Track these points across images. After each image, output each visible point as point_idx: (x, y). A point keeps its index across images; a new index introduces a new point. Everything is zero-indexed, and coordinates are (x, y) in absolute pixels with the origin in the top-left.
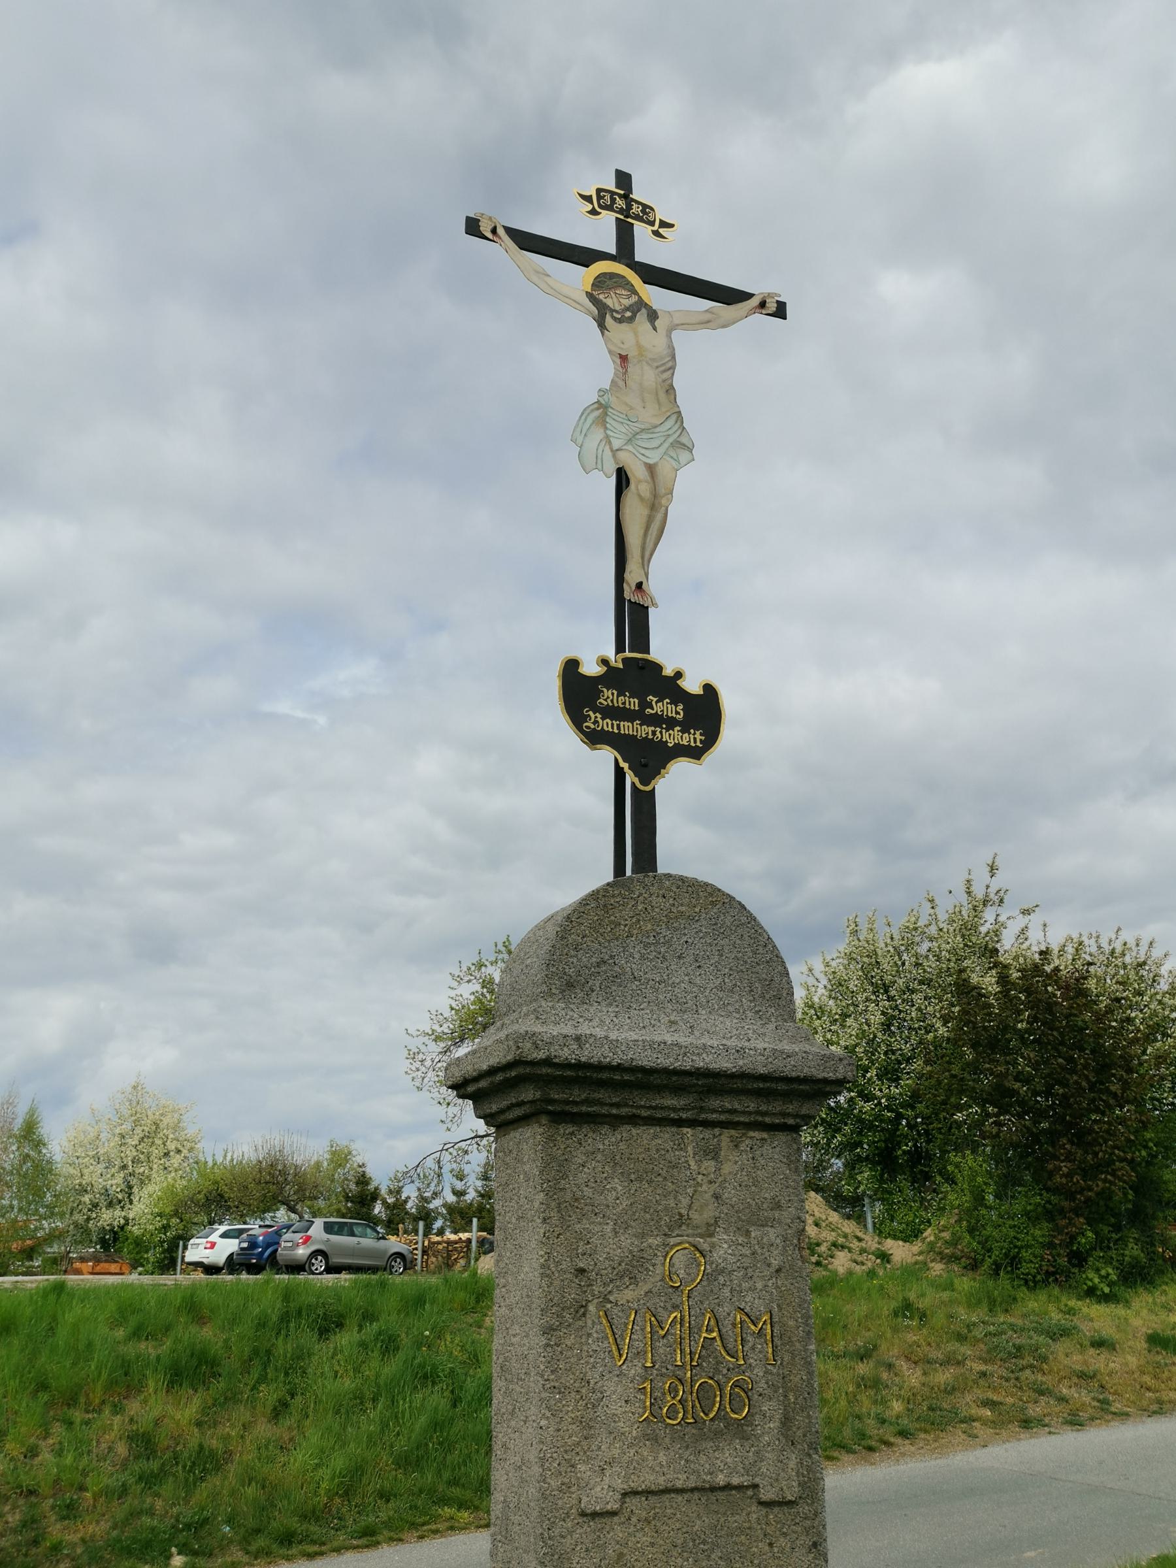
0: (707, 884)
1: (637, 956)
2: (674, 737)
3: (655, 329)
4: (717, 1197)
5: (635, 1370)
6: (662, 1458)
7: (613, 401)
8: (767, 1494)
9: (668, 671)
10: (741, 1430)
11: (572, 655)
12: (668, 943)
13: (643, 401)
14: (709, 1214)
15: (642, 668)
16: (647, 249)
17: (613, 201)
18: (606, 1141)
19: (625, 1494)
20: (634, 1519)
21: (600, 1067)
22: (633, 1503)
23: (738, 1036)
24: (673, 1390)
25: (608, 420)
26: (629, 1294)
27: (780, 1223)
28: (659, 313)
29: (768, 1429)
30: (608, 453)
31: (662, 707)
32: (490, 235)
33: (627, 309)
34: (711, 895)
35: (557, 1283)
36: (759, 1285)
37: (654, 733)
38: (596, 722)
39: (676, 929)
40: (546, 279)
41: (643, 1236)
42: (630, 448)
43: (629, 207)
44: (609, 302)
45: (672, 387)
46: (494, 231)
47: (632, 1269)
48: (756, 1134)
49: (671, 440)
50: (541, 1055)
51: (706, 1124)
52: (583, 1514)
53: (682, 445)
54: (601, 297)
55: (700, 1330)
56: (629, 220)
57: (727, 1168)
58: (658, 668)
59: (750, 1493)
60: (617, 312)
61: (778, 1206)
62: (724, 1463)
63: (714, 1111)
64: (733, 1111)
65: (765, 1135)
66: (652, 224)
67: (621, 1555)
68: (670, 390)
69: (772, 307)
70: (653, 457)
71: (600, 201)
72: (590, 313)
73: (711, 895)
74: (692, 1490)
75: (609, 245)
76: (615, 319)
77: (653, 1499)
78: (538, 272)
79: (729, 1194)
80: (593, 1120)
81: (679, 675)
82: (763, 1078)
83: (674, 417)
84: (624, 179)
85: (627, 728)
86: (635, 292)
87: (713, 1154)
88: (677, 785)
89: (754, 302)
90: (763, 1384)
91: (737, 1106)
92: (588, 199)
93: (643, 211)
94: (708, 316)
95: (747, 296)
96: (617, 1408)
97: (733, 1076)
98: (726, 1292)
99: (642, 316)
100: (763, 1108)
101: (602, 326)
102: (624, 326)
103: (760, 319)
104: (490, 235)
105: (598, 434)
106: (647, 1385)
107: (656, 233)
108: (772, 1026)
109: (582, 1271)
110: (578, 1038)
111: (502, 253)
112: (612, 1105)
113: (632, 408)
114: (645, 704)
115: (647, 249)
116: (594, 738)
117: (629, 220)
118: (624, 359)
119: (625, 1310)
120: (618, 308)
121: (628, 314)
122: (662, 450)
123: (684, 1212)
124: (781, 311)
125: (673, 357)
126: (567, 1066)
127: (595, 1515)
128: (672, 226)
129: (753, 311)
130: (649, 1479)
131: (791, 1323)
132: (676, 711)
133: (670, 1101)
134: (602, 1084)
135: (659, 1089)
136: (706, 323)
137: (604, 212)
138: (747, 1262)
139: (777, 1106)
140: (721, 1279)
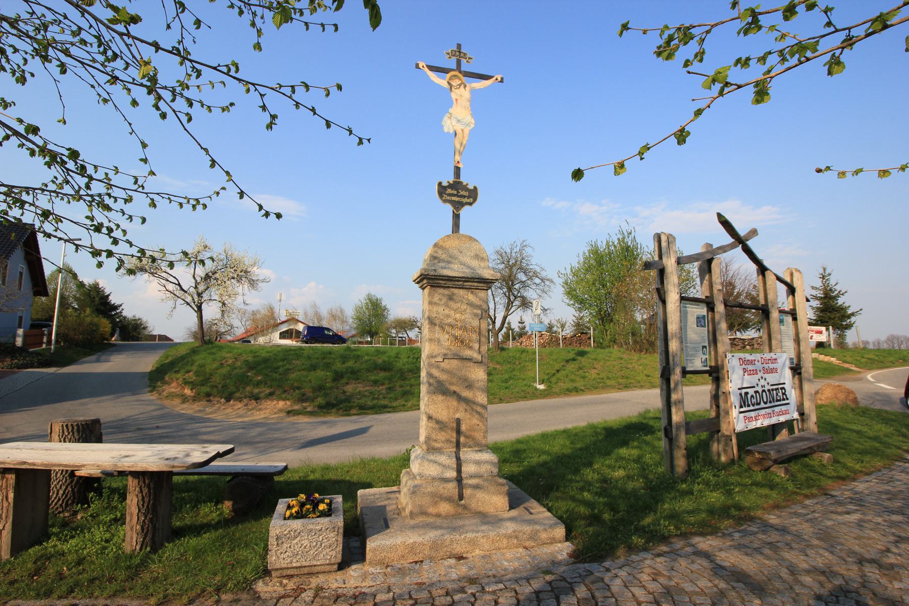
2: (465, 200)
16: (464, 68)
71: (453, 54)
75: (454, 66)
84: (459, 46)
85: (453, 198)
88: (465, 212)
116: (445, 201)
132: (466, 194)
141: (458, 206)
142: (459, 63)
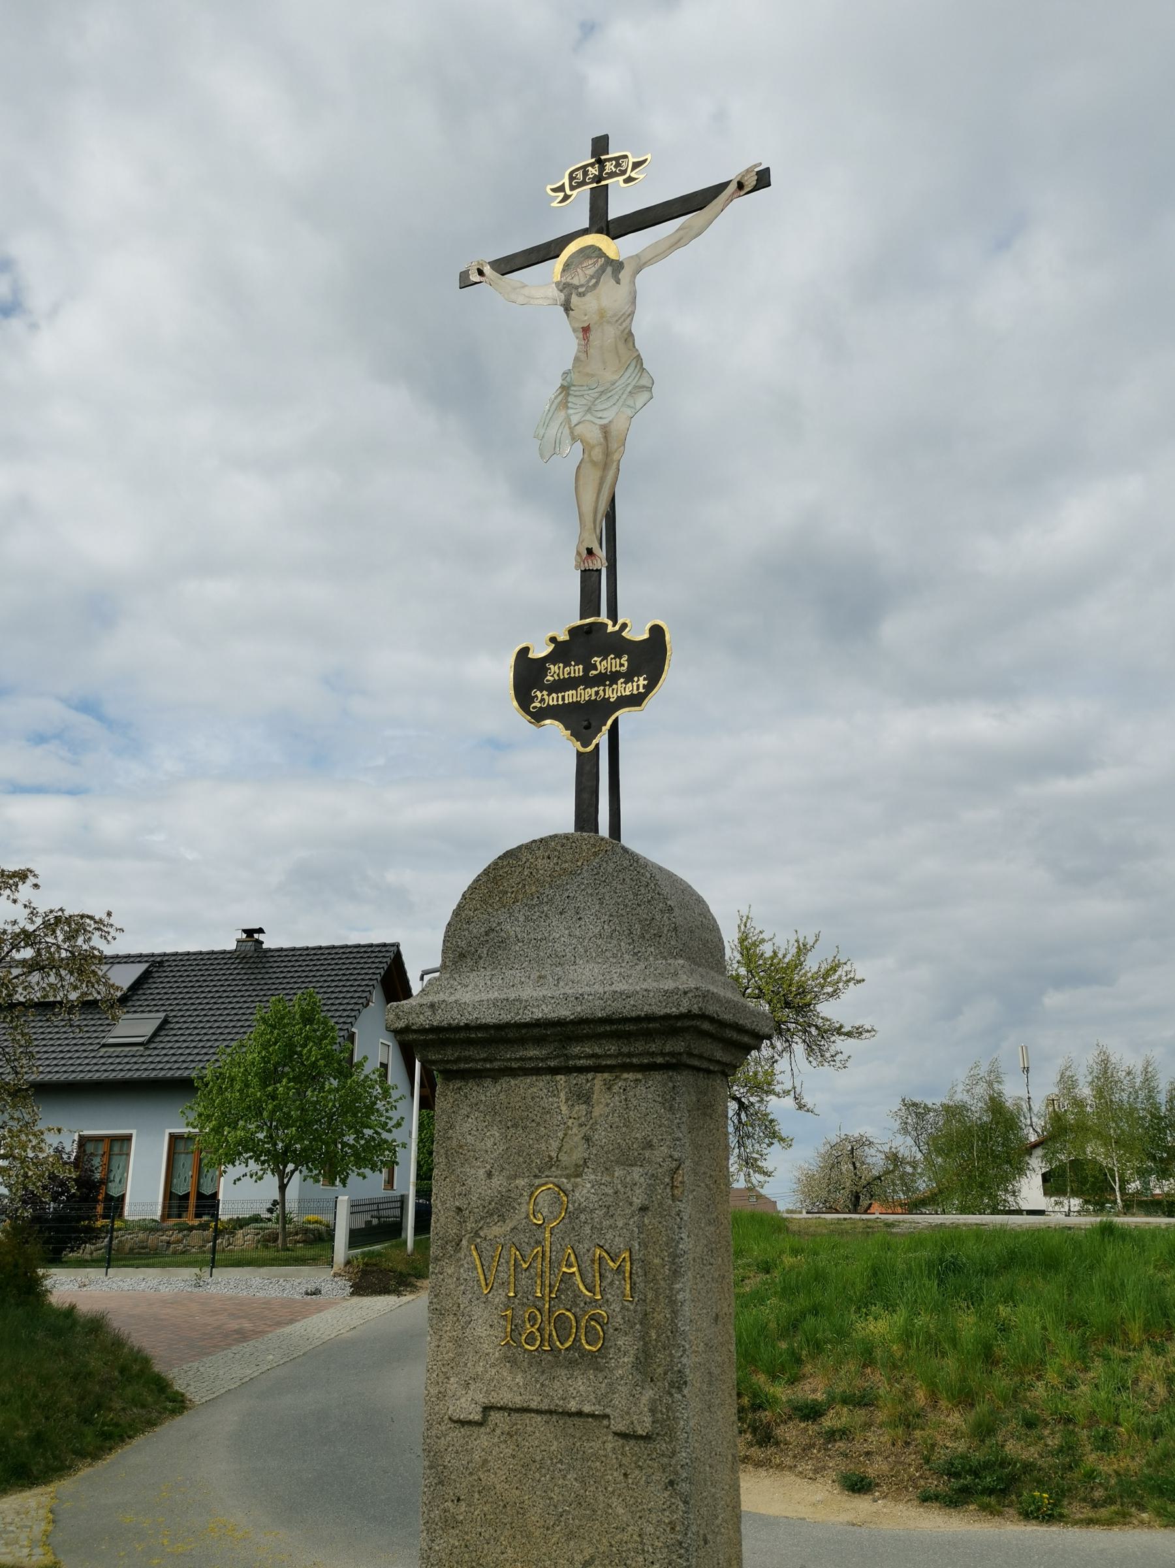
2: (612, 693)
3: (618, 282)
4: (587, 1139)
5: (499, 1298)
8: (621, 1427)
10: (595, 1362)
14: (579, 1154)
17: (585, 174)
18: (489, 1092)
20: (498, 1432)
21: (451, 1029)
22: (495, 1416)
26: (496, 1230)
29: (623, 1362)
31: (603, 665)
33: (592, 277)
36: (620, 1224)
38: (543, 700)
39: (558, 887)
41: (515, 1177)
45: (631, 334)
47: (501, 1207)
48: (630, 1076)
49: (629, 389)
56: (603, 183)
57: (597, 1112)
59: (605, 1422)
60: (582, 286)
61: (649, 1145)
62: (578, 1391)
64: (594, 1056)
65: (639, 1076)
67: (485, 1461)
68: (629, 337)
69: (751, 181)
70: (608, 416)
77: (515, 1416)
79: (600, 1136)
80: (477, 1075)
84: (600, 145)
85: (570, 696)
87: (584, 1097)
89: (733, 187)
90: (619, 1319)
91: (598, 1050)
93: (618, 165)
95: (723, 186)
97: (572, 1022)
100: (625, 1050)
109: (459, 1209)
114: (590, 667)
116: (538, 716)
117: (603, 183)
120: (583, 281)
121: (594, 281)
123: (554, 1154)
124: (763, 179)
130: (505, 1397)
131: (657, 1261)
132: (621, 664)
133: (532, 1052)
134: (470, 1042)
135: (522, 1042)
136: (677, 243)
137: (575, 193)
139: (639, 1046)
140: (583, 1217)
141: (585, 721)
142: (599, 199)
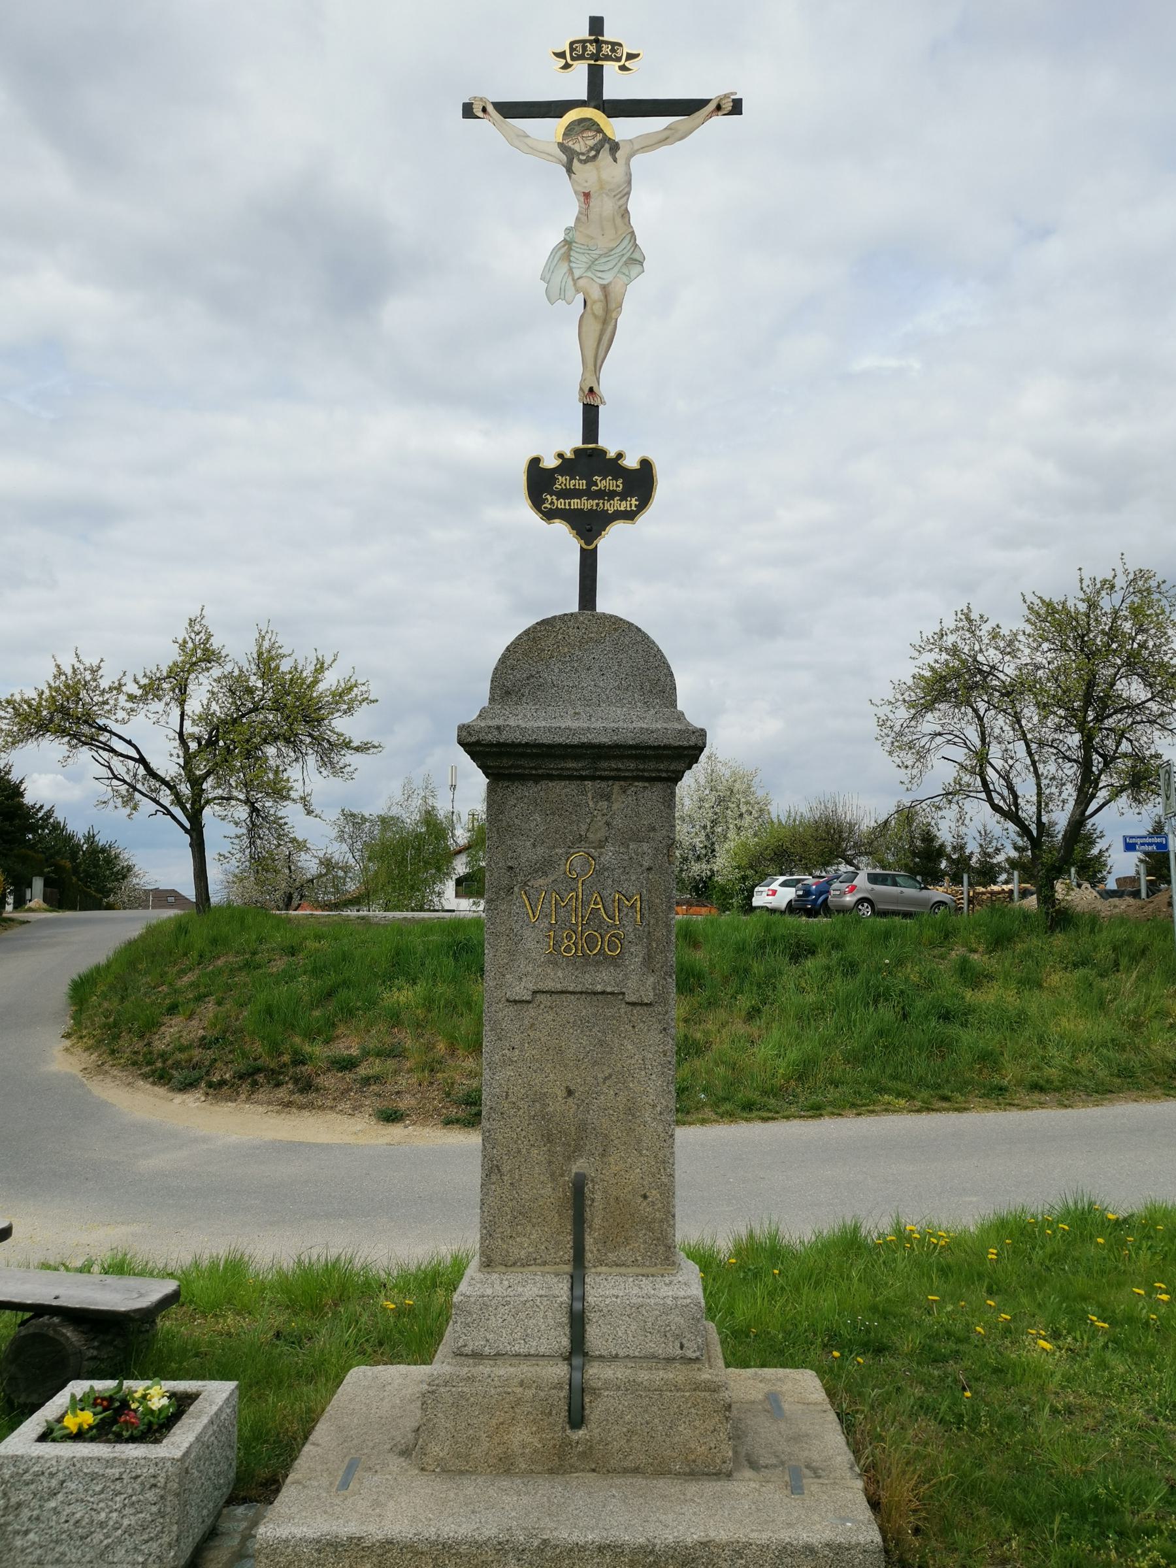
0: (611, 616)
1: (556, 671)
3: (615, 161)
4: (608, 824)
5: (544, 924)
6: (560, 974)
7: (579, 238)
8: (633, 999)
9: (612, 454)
10: (615, 962)
11: (534, 455)
12: (580, 660)
13: (603, 229)
14: (601, 835)
15: (590, 456)
16: (610, 92)
17: (584, 48)
18: (530, 790)
19: (535, 992)
20: (542, 1006)
21: (514, 745)
22: (539, 997)
23: (624, 720)
24: (569, 937)
25: (572, 253)
26: (541, 881)
27: (653, 840)
28: (621, 145)
29: (634, 962)
30: (570, 283)
31: (603, 483)
32: (480, 114)
33: (592, 149)
34: (614, 623)
35: (496, 875)
36: (633, 878)
37: (597, 505)
38: (552, 503)
39: (586, 650)
40: (527, 140)
41: (554, 847)
42: (589, 274)
43: (599, 49)
44: (577, 147)
45: (627, 211)
46: (484, 110)
47: (544, 867)
48: (640, 784)
49: (624, 259)
50: (473, 739)
51: (602, 778)
52: (508, 1001)
53: (635, 261)
54: (570, 144)
55: (589, 903)
56: (599, 63)
57: (615, 807)
58: (603, 452)
59: (621, 997)
60: (583, 154)
61: (654, 829)
62: (604, 979)
63: (605, 770)
64: (618, 770)
65: (647, 784)
66: (619, 59)
67: (533, 1025)
68: (625, 214)
69: (728, 106)
70: (608, 278)
71: (577, 51)
72: (560, 162)
73: (614, 623)
74: (581, 993)
75: (580, 92)
76: (580, 161)
77: (554, 996)
78: (518, 136)
79: (618, 822)
80: (522, 778)
81: (620, 456)
82: (631, 747)
83: (628, 237)
84: (596, 24)
85: (576, 503)
86: (600, 131)
87: (608, 797)
88: (614, 541)
89: (711, 106)
90: (632, 936)
91: (620, 766)
92: (561, 55)
93: (613, 50)
94: (668, 133)
95: (705, 102)
96: (531, 945)
97: (609, 747)
98: (610, 882)
99: (605, 154)
100: (641, 767)
101: (570, 171)
102: (589, 166)
103: (719, 121)
104: (480, 114)
105: (564, 268)
106: (552, 933)
107: (623, 68)
108: (652, 712)
109: (511, 868)
110: (498, 728)
111: (487, 127)
112: (531, 768)
113: (592, 238)
114: (592, 483)
115: (616, 86)
116: (549, 515)
117: (599, 63)
118: (587, 195)
119: (538, 890)
120: (584, 150)
121: (593, 153)
122: (616, 269)
123: (583, 833)
124: (737, 108)
125: (629, 182)
126: (491, 745)
127: (516, 1002)
128: (638, 55)
129: (710, 116)
130: (550, 985)
131: (657, 901)
132: (618, 485)
133: (570, 765)
134: (523, 755)
135: (564, 757)
136: (665, 139)
137: (575, 63)
138: (625, 864)
139: (652, 765)
140: (606, 874)
141: (589, 527)
142: (595, 78)
